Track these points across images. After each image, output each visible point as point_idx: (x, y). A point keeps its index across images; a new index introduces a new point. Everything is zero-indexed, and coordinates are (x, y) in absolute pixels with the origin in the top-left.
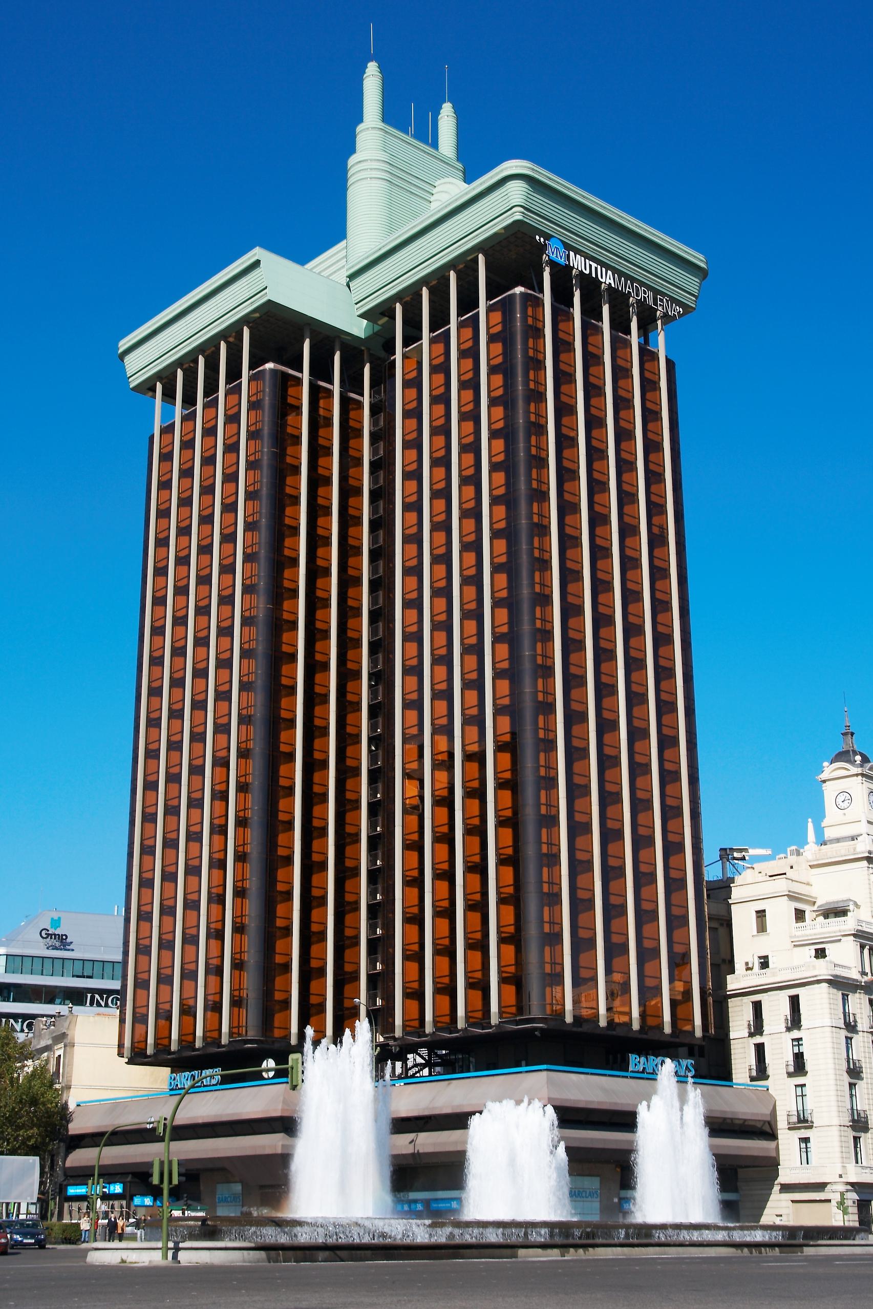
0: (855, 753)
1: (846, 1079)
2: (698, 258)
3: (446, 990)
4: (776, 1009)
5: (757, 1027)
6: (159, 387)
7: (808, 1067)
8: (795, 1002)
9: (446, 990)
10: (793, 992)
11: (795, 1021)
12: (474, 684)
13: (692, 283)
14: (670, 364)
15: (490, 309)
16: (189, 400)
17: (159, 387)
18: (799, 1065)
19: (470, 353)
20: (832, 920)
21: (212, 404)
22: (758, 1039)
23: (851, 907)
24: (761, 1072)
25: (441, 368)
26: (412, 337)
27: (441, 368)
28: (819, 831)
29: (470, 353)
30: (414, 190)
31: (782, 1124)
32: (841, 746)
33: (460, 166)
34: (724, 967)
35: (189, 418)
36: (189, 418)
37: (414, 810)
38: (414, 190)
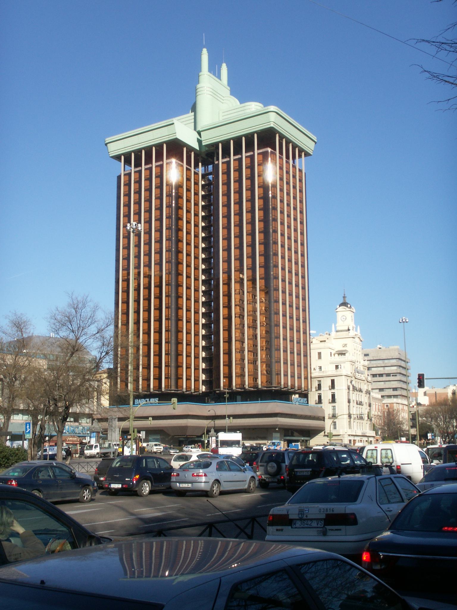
1: (348, 404)
2: (315, 138)
4: (326, 384)
5: (319, 387)
7: (336, 401)
8: (333, 382)
10: (333, 378)
11: (333, 386)
18: (333, 400)
22: (319, 392)
24: (320, 401)
28: (335, 327)
31: (326, 418)
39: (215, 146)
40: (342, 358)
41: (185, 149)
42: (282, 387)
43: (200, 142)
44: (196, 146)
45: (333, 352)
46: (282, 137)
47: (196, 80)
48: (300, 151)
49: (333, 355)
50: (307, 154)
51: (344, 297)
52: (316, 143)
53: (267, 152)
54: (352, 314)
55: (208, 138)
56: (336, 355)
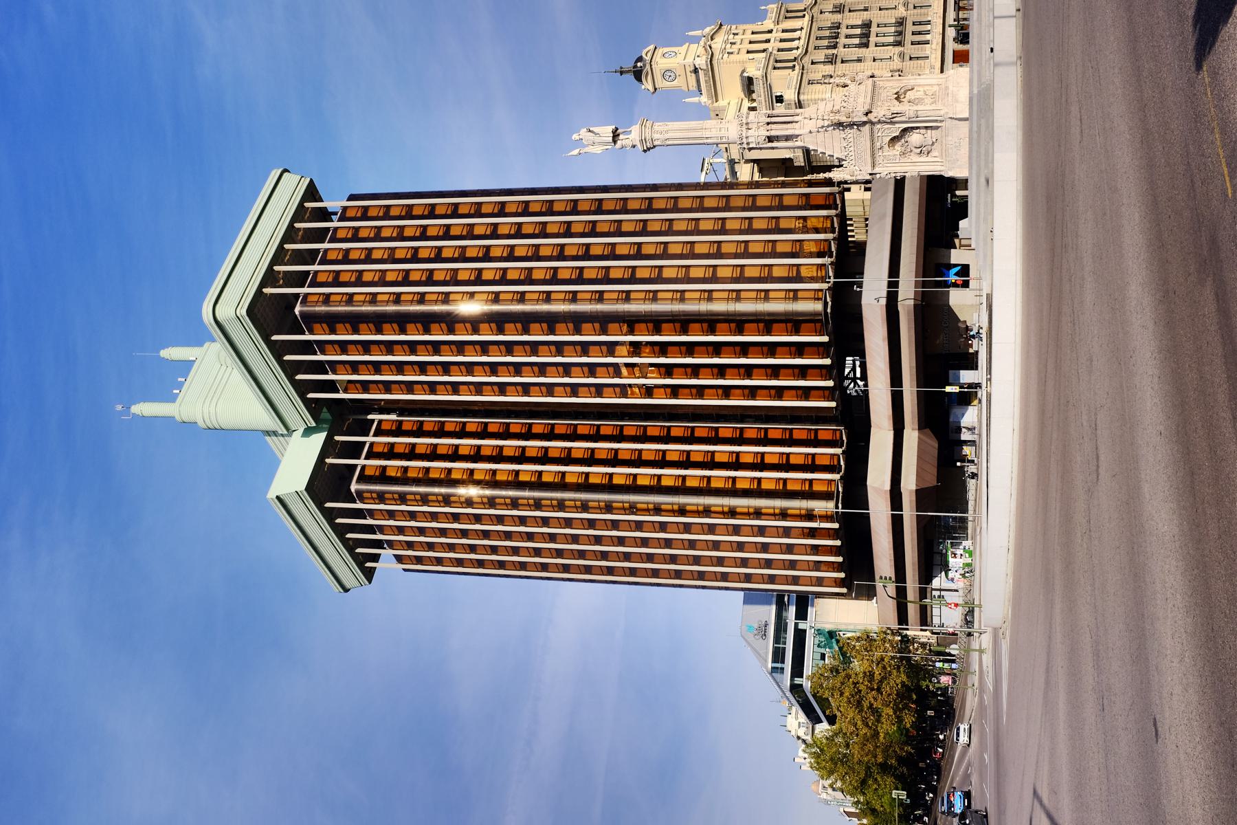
0: (635, 66)
2: (275, 174)
3: (803, 372)
6: (368, 564)
9: (803, 372)
12: (585, 348)
13: (290, 180)
14: (352, 198)
15: (311, 333)
16: (378, 544)
17: (368, 564)
19: (343, 347)
20: (755, 88)
21: (381, 529)
23: (745, 74)
25: (354, 367)
26: (331, 386)
27: (354, 367)
28: (690, 94)
29: (343, 347)
30: (224, 381)
32: (631, 77)
33: (207, 345)
34: (788, 164)
35: (391, 544)
36: (391, 544)
37: (675, 391)
38: (224, 381)
39: (314, 408)
40: (759, 87)
41: (328, 461)
42: (825, 286)
43: (308, 432)
44: (319, 438)
45: (746, 104)
46: (270, 278)
47: (189, 426)
48: (310, 205)
49: (754, 105)
50: (312, 193)
51: (622, 73)
52: (286, 171)
53: (301, 313)
54: (660, 51)
55: (297, 415)
56: (754, 96)
